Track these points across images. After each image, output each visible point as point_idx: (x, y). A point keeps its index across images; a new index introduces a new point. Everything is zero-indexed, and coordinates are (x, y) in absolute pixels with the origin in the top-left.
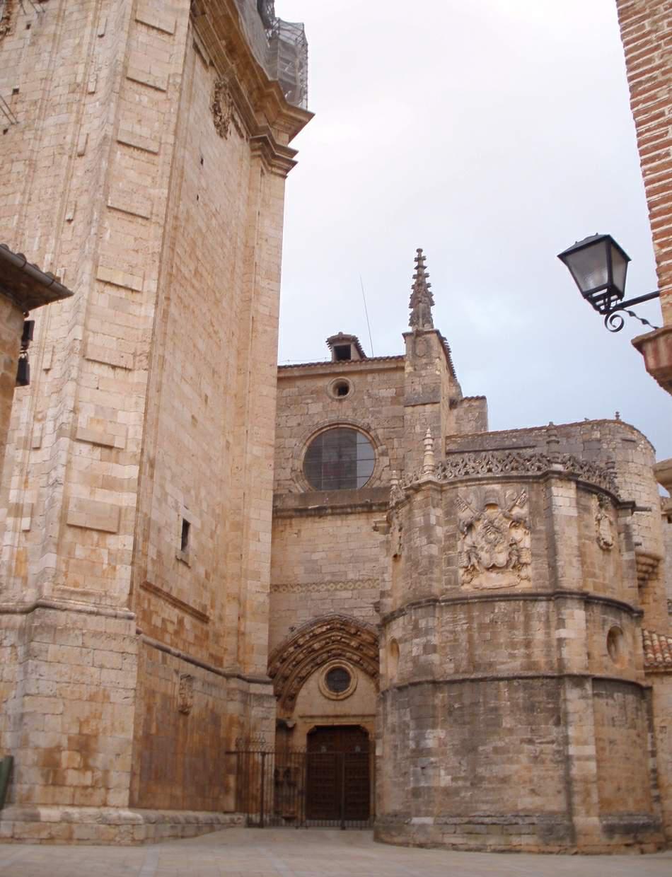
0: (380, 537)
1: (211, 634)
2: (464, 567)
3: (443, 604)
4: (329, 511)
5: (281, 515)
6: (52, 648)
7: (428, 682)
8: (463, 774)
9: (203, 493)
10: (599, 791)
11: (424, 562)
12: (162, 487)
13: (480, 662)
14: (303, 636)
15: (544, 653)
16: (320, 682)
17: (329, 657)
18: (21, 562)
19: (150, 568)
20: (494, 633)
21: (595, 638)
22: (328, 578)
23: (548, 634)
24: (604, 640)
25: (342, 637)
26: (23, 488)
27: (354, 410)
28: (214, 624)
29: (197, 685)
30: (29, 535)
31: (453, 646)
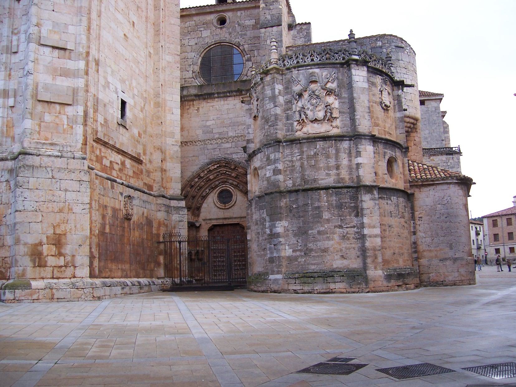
0: (245, 107)
1: (144, 170)
2: (297, 121)
3: (284, 144)
4: (216, 95)
5: (185, 100)
6: (31, 180)
7: (276, 192)
8: (299, 248)
9: (134, 84)
10: (382, 255)
11: (273, 118)
12: (105, 78)
13: (309, 178)
14: (203, 171)
15: (348, 172)
16: (214, 198)
17: (219, 183)
18: (10, 128)
19: (99, 129)
20: (316, 161)
21: (380, 163)
22: (217, 136)
23: (350, 161)
24: (385, 165)
25: (227, 171)
26: (7, 79)
27: (230, 34)
28: (146, 165)
29: (135, 202)
30: (14, 109)
31: (292, 170)
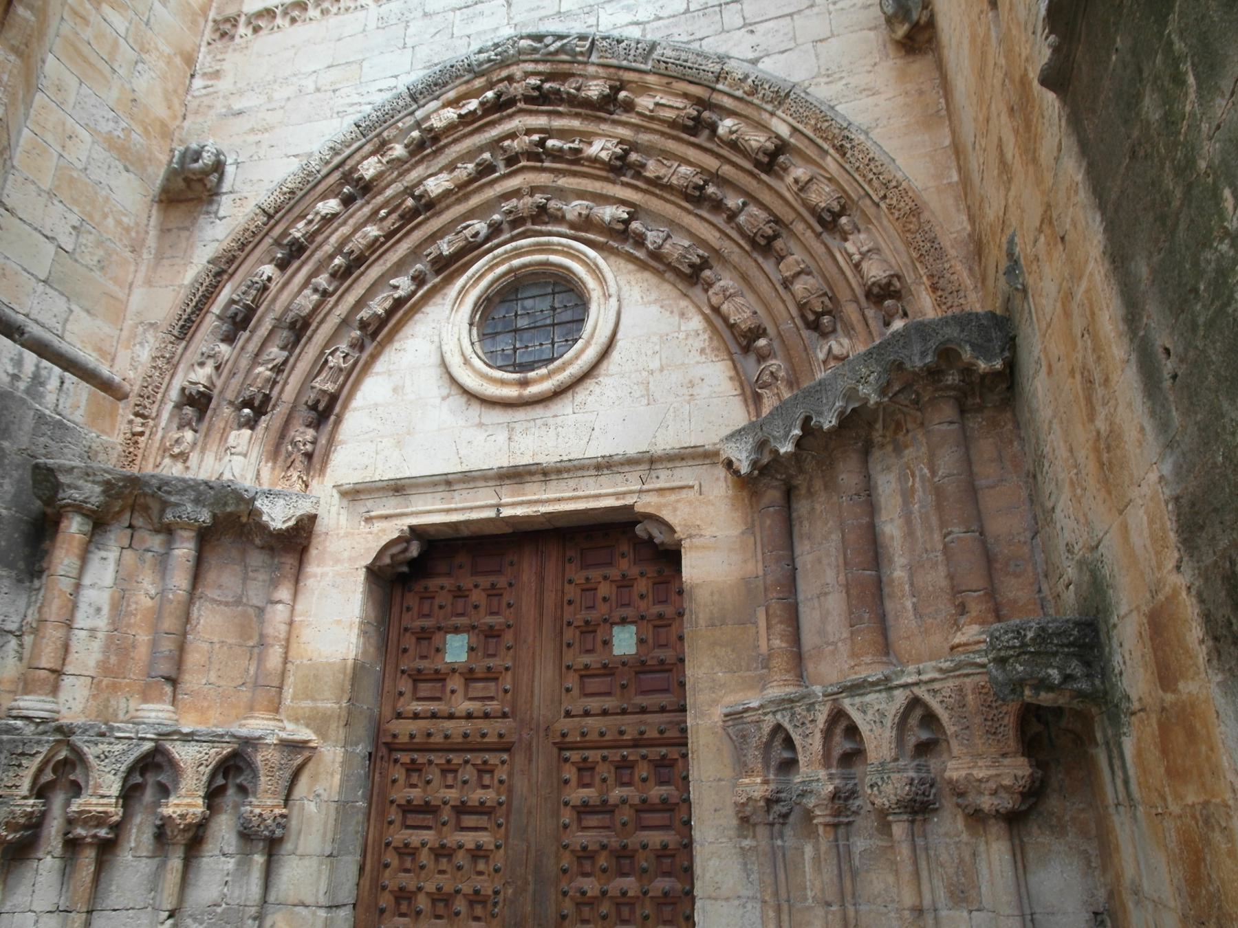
25: (549, 133)
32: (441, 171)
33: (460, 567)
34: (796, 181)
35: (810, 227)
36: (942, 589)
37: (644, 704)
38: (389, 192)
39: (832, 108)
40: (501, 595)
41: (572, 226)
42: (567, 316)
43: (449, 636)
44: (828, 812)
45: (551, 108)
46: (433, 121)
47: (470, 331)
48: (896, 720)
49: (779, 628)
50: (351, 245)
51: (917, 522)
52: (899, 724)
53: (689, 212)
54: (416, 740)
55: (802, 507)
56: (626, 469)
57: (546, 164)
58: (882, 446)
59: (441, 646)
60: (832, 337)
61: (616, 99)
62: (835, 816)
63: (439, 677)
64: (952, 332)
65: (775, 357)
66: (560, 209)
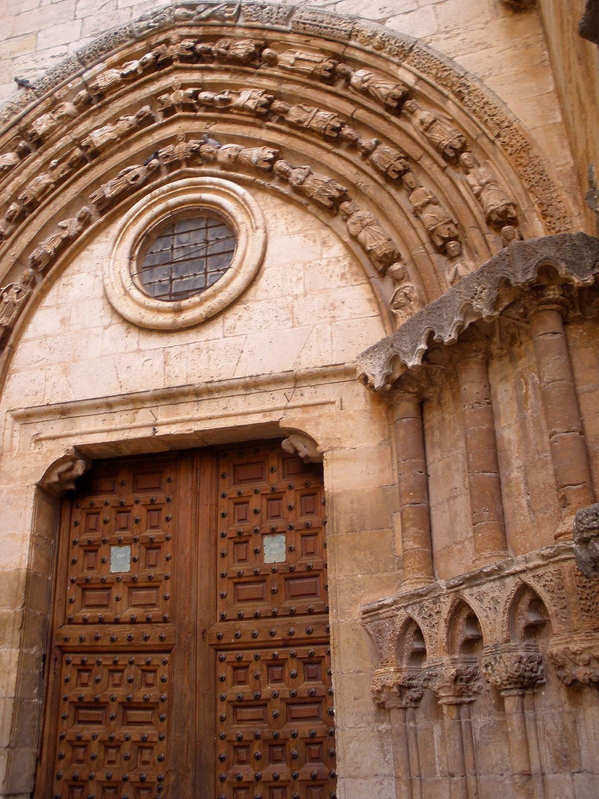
25: (203, 87)
32: (105, 124)
33: (123, 484)
34: (422, 123)
35: (435, 162)
36: (550, 486)
37: (293, 608)
38: (59, 144)
39: (451, 59)
40: (160, 510)
41: (224, 166)
42: (219, 248)
43: (113, 549)
44: (451, 693)
45: (203, 65)
46: (98, 81)
47: (130, 264)
48: (508, 606)
49: (412, 531)
50: (25, 192)
51: (530, 426)
52: (510, 609)
53: (329, 151)
54: (86, 643)
55: (433, 417)
56: (273, 387)
57: (200, 114)
58: (501, 357)
59: (106, 558)
60: (458, 259)
61: (261, 56)
62: (458, 696)
63: (105, 586)
64: (550, 252)
65: (409, 280)
66: (211, 152)
